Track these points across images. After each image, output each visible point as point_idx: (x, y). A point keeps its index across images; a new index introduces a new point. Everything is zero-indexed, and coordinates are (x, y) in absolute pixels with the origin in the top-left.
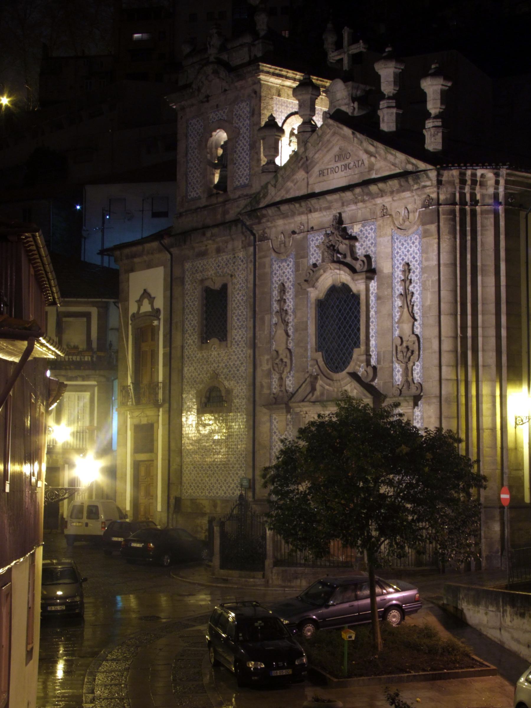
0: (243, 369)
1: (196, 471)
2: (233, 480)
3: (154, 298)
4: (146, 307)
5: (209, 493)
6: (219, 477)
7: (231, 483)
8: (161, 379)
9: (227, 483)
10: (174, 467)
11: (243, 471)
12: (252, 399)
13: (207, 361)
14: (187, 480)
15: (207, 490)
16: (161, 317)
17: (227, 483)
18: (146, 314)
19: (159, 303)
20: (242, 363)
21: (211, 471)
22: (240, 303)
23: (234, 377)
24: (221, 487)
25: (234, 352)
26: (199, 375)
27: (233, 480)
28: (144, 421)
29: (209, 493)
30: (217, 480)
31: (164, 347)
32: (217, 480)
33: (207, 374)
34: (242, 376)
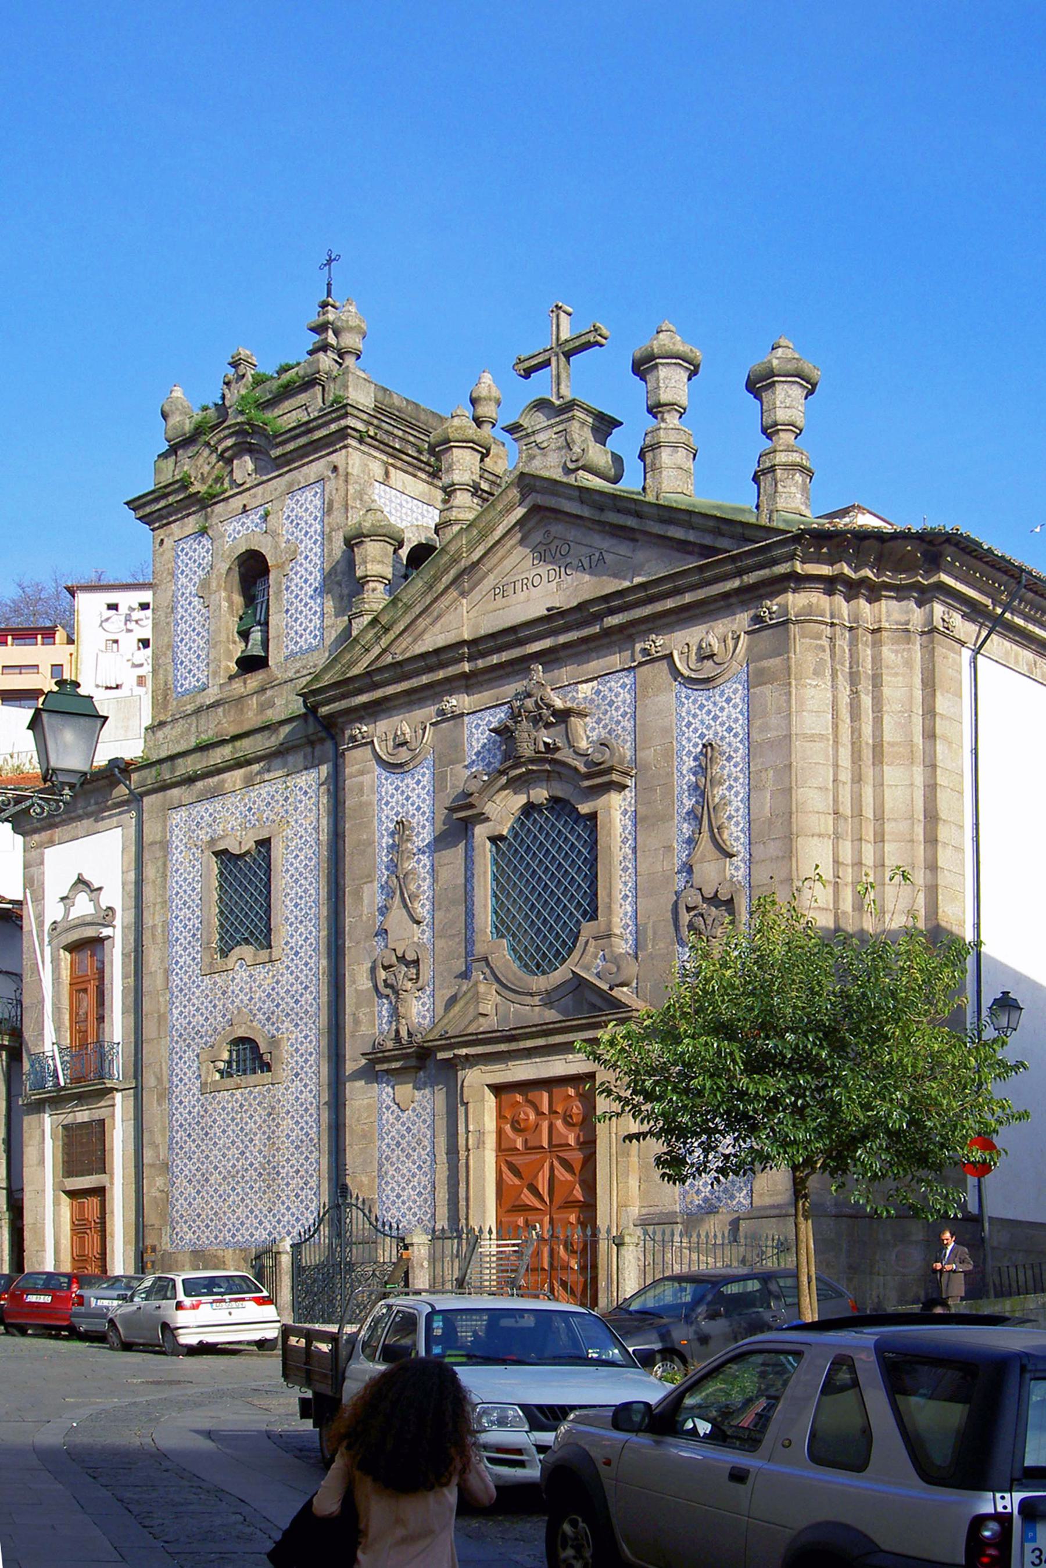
0: (310, 998)
1: (203, 1198)
2: (288, 1208)
3: (100, 889)
4: (83, 906)
5: (234, 1236)
6: (256, 1205)
7: (283, 1215)
8: (118, 1037)
9: (274, 1216)
10: (151, 1192)
11: (311, 1189)
12: (333, 1051)
13: (224, 993)
14: (182, 1216)
15: (229, 1230)
16: (118, 922)
17: (274, 1216)
18: (84, 923)
19: (114, 896)
20: (306, 988)
21: (238, 1194)
22: (301, 874)
23: (288, 1015)
24: (261, 1223)
25: (288, 967)
26: (207, 1019)
27: (288, 1208)
28: (83, 1116)
29: (234, 1236)
30: (252, 1211)
31: (125, 977)
32: (252, 1211)
33: (224, 1015)
34: (306, 1012)
